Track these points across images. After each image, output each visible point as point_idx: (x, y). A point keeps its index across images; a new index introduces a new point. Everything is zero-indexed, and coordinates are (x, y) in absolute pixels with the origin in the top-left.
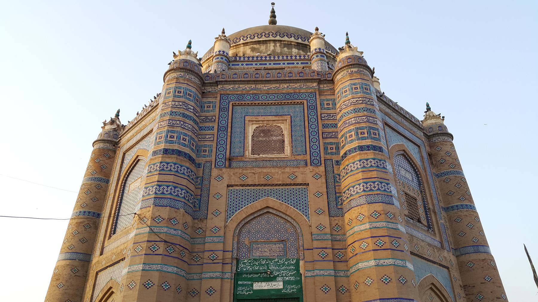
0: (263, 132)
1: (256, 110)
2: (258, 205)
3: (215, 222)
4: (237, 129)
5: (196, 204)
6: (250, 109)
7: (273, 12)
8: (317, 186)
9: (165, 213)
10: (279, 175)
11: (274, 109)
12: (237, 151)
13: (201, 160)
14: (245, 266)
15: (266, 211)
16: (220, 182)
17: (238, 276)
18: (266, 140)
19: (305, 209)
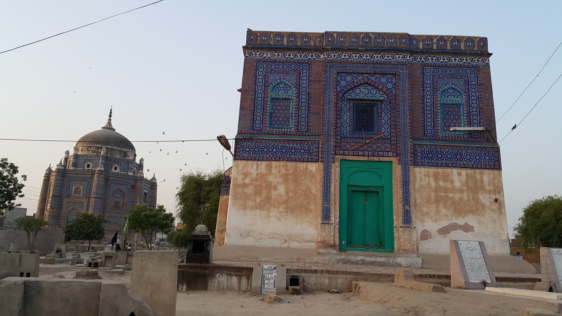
0: (77, 188)
1: (76, 182)
2: (73, 207)
3: (64, 211)
4: (71, 188)
5: (60, 207)
6: (74, 182)
7: (111, 111)
8: (86, 204)
9: (52, 210)
10: (78, 201)
11: (80, 182)
12: (70, 194)
13: (62, 195)
14: (69, 220)
15: (74, 209)
16: (65, 201)
17: (68, 222)
18: (77, 191)
19: (82, 209)
